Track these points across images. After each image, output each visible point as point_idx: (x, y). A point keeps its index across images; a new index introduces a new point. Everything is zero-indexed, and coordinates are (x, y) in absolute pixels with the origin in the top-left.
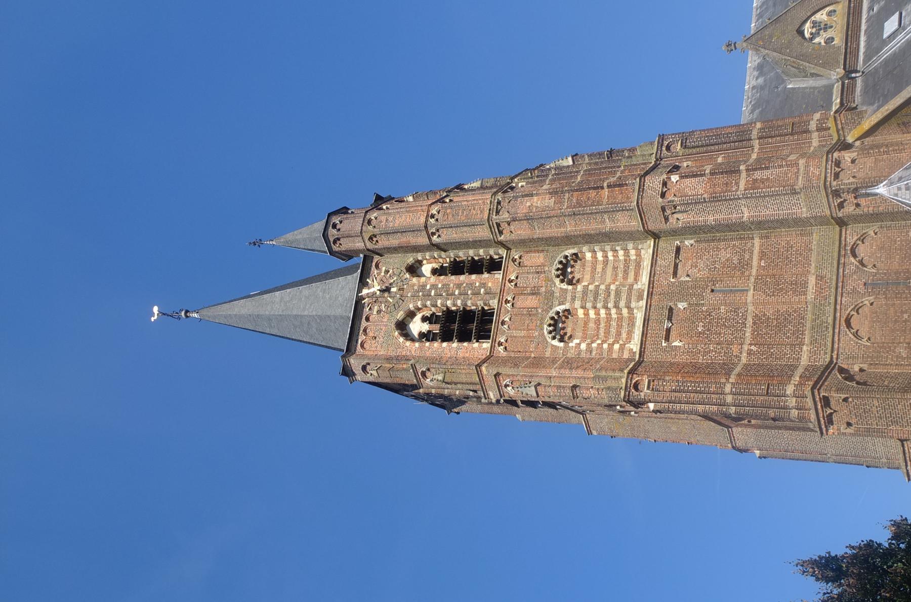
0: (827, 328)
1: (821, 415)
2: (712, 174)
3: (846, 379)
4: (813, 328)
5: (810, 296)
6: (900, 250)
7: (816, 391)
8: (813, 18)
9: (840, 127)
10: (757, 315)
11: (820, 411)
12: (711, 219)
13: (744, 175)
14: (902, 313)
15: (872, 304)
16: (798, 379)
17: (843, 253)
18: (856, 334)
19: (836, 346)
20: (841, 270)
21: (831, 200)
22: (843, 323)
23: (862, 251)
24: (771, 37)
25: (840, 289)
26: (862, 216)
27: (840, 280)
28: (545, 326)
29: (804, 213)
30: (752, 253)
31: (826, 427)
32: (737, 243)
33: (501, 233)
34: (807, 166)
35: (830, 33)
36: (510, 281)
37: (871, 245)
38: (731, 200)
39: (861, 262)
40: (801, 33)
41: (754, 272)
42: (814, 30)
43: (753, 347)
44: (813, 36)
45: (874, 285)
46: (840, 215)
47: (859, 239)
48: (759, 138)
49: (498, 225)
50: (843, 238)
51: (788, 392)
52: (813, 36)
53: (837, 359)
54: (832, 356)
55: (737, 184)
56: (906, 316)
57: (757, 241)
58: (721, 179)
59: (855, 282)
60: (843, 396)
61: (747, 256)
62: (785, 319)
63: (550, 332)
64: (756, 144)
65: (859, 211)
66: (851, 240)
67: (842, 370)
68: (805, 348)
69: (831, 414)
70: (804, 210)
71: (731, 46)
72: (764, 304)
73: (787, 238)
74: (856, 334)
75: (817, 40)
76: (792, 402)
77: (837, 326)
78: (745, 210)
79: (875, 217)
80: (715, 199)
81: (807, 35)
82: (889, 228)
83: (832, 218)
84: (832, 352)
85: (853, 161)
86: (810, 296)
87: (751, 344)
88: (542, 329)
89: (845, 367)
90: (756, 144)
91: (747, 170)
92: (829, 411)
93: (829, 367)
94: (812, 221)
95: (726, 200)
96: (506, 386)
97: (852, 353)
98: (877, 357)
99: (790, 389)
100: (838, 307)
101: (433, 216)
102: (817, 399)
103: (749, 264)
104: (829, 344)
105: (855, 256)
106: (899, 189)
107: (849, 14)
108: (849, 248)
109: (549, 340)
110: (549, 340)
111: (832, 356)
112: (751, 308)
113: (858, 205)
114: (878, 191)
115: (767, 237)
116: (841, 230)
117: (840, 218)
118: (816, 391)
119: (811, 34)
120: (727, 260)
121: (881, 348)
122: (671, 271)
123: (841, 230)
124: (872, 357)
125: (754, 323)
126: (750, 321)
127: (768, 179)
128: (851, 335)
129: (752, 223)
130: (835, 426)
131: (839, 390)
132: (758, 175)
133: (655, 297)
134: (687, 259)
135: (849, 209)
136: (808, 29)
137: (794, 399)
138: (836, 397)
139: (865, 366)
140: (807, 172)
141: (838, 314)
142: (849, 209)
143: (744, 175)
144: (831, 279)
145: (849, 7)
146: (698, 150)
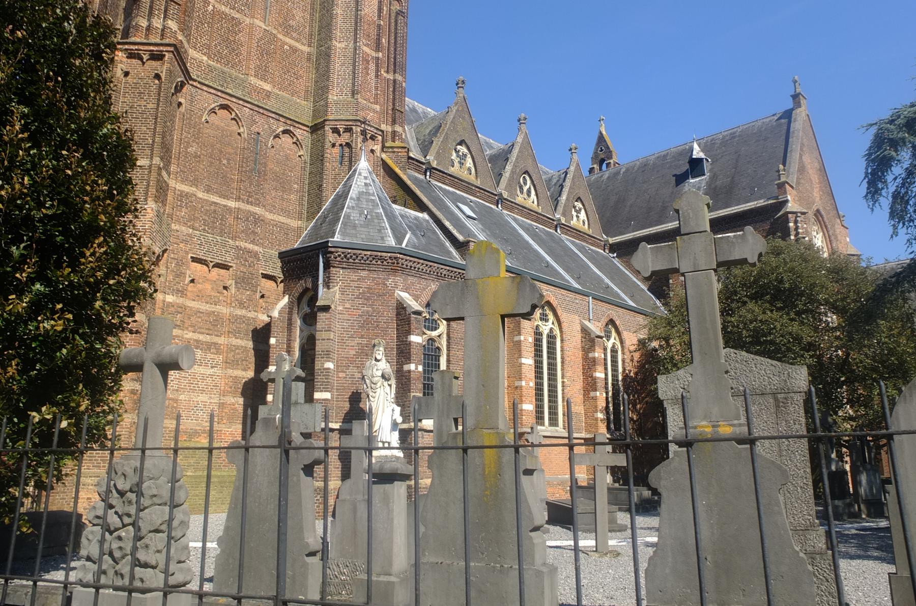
0: (223, 86)
2: (379, 26)
3: (176, 87)
4: (223, 73)
5: (253, 80)
6: (283, 174)
7: (172, 49)
8: (469, 156)
9: (396, 150)
10: (241, 24)
11: (146, 48)
12: (338, 11)
13: (374, 54)
14: (228, 160)
15: (239, 134)
16: (180, 38)
17: (289, 122)
18: (213, 111)
19: (205, 88)
20: (273, 115)
21: (343, 123)
22: (226, 102)
23: (286, 139)
24: (463, 118)
25: (257, 109)
26: (323, 147)
27: (265, 112)
29: (332, 97)
30: (296, 40)
31: (126, 50)
32: (307, 30)
34: (374, 111)
35: (457, 164)
37: (291, 150)
38: (356, 34)
39: (277, 136)
40: (460, 144)
41: (280, 36)
43: (210, 8)
44: (457, 152)
45: (257, 141)
46: (327, 128)
47: (298, 140)
48: (395, 81)
50: (301, 126)
51: (170, 22)
52: (457, 152)
53: (192, 85)
54: (195, 81)
55: (367, 45)
56: (225, 162)
57: (306, 49)
58: (373, 33)
59: (262, 125)
60: (163, 76)
61: (294, 35)
62: (233, 49)
64: (390, 76)
65: (328, 145)
66: (298, 132)
67: (182, 85)
68: (205, 58)
69: (141, 59)
70: (335, 98)
71: (460, 84)
72: (250, 35)
73: (306, 78)
74: (213, 111)
75: (454, 154)
76: (157, 23)
77: (223, 95)
78: (343, 45)
79: (318, 158)
80: (357, 21)
81: (459, 147)
82: (304, 169)
83: (325, 120)
84: (199, 82)
85: (372, 151)
86: (253, 80)
87: (214, 6)
89: (184, 90)
90: (390, 76)
91: (378, 58)
92: (145, 57)
93: (186, 73)
94: (322, 103)
95: (356, 30)
97: (197, 101)
98: (189, 124)
99: (172, 25)
100: (241, 102)
103: (287, 34)
104: (207, 83)
105: (285, 132)
106: (366, 178)
107: (469, 183)
108: (292, 129)
111: (195, 81)
112: (248, 21)
113: (334, 145)
114: (363, 158)
115: (309, 59)
116: (307, 126)
117: (323, 127)
118: (172, 49)
120: (293, 15)
121: (199, 130)
123: (307, 126)
124: (190, 119)
125: (233, 18)
126: (237, 16)
127: (368, 74)
128: (213, 106)
129: (329, 48)
130: (125, 60)
131: (170, 72)
132: (372, 66)
135: (331, 137)
136: (463, 149)
137: (161, 27)
138: (163, 68)
139: (182, 109)
140: (369, 109)
141: (234, 100)
142: (331, 137)
143: (374, 54)
144: (266, 104)
145: (473, 185)
146: (393, 24)
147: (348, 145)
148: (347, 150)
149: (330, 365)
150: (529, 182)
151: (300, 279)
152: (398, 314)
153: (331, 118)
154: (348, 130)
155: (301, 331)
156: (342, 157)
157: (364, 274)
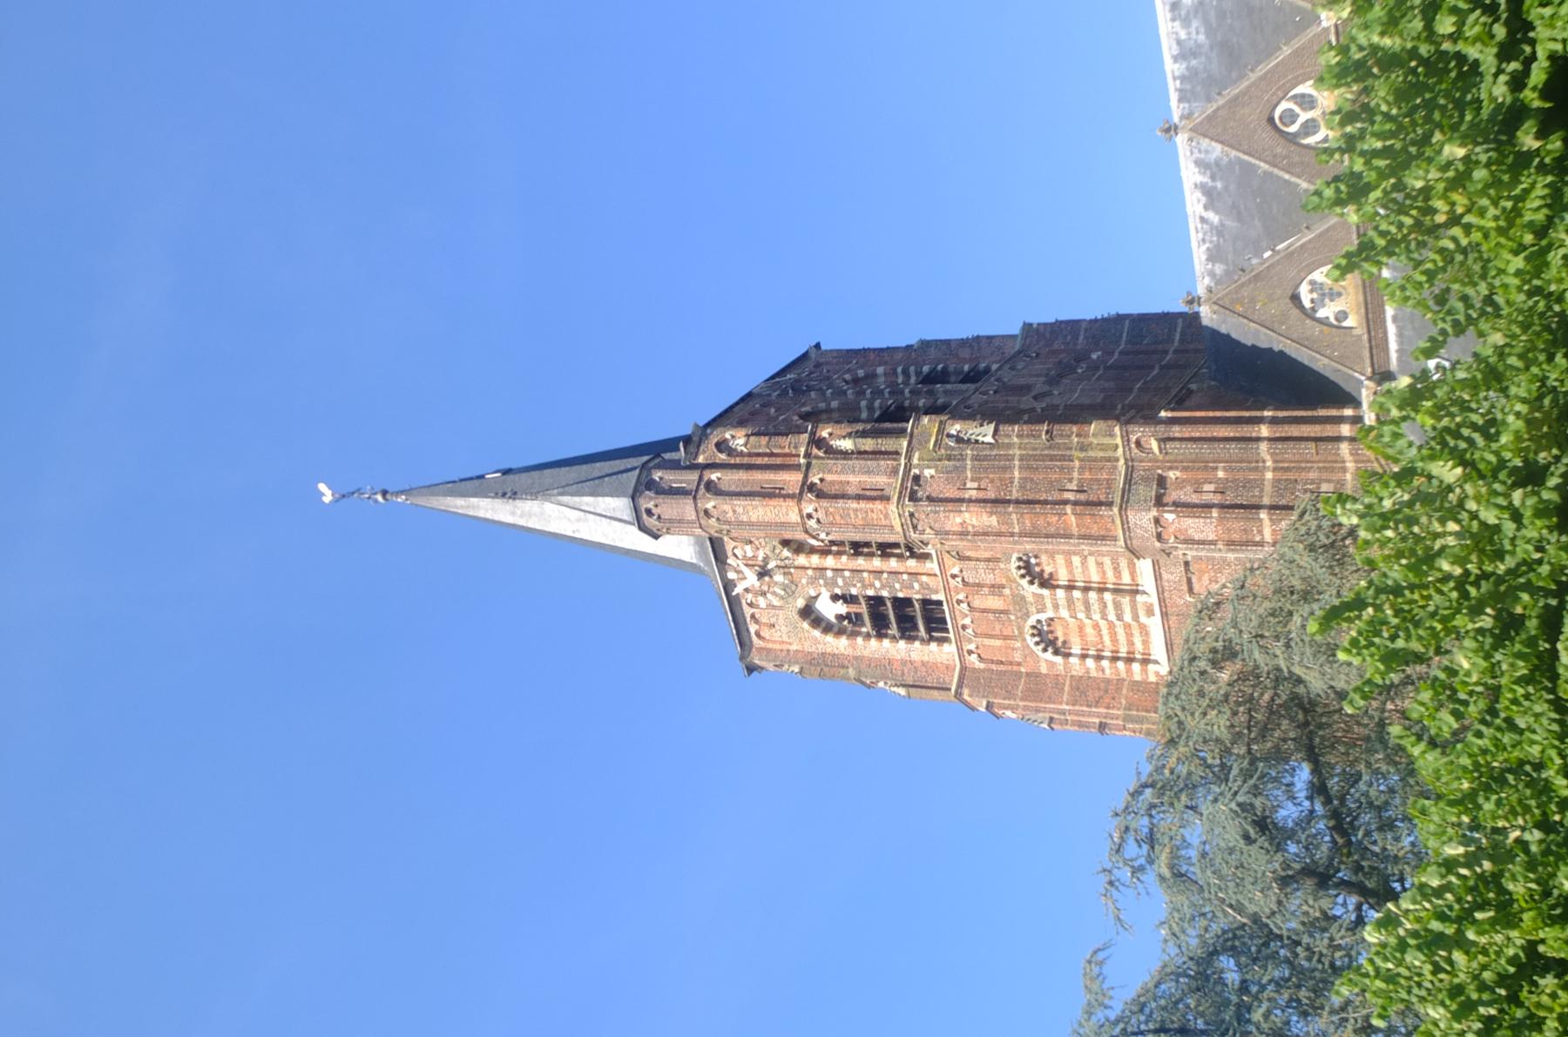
28: (1028, 638)
36: (954, 576)
40: (1296, 298)
42: (1315, 296)
63: (1037, 643)
81: (1307, 304)
88: (1024, 640)
101: (810, 516)
107: (1364, 287)
109: (1040, 654)
110: (1040, 654)
119: (1312, 301)
122: (1185, 587)
133: (1173, 619)
134: (1202, 572)
150: (1284, 105)
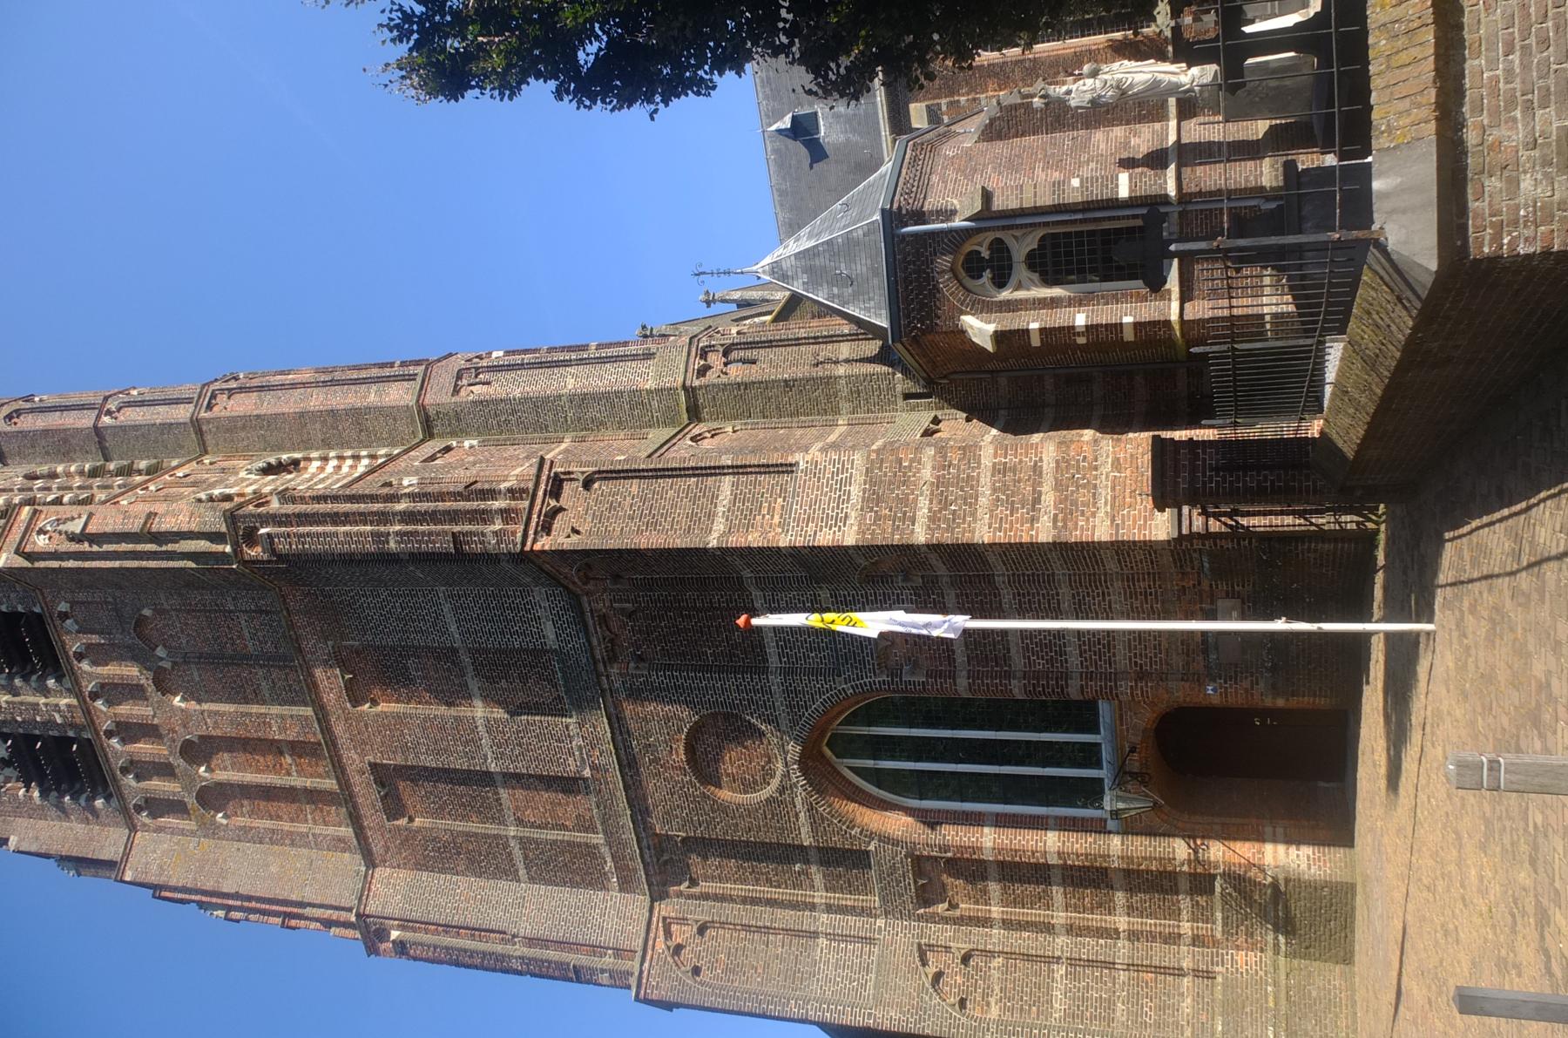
1: (537, 509)
33: (210, 407)
46: (696, 383)
49: (213, 396)
65: (724, 379)
96: (41, 531)
102: (544, 478)
129: (572, 398)
135: (711, 377)
147: (725, 354)
148: (734, 355)
149: (1076, 182)
151: (936, 288)
152: (1000, 137)
153: (680, 380)
154: (704, 353)
155: (1019, 287)
156: (744, 361)
157: (935, 179)
